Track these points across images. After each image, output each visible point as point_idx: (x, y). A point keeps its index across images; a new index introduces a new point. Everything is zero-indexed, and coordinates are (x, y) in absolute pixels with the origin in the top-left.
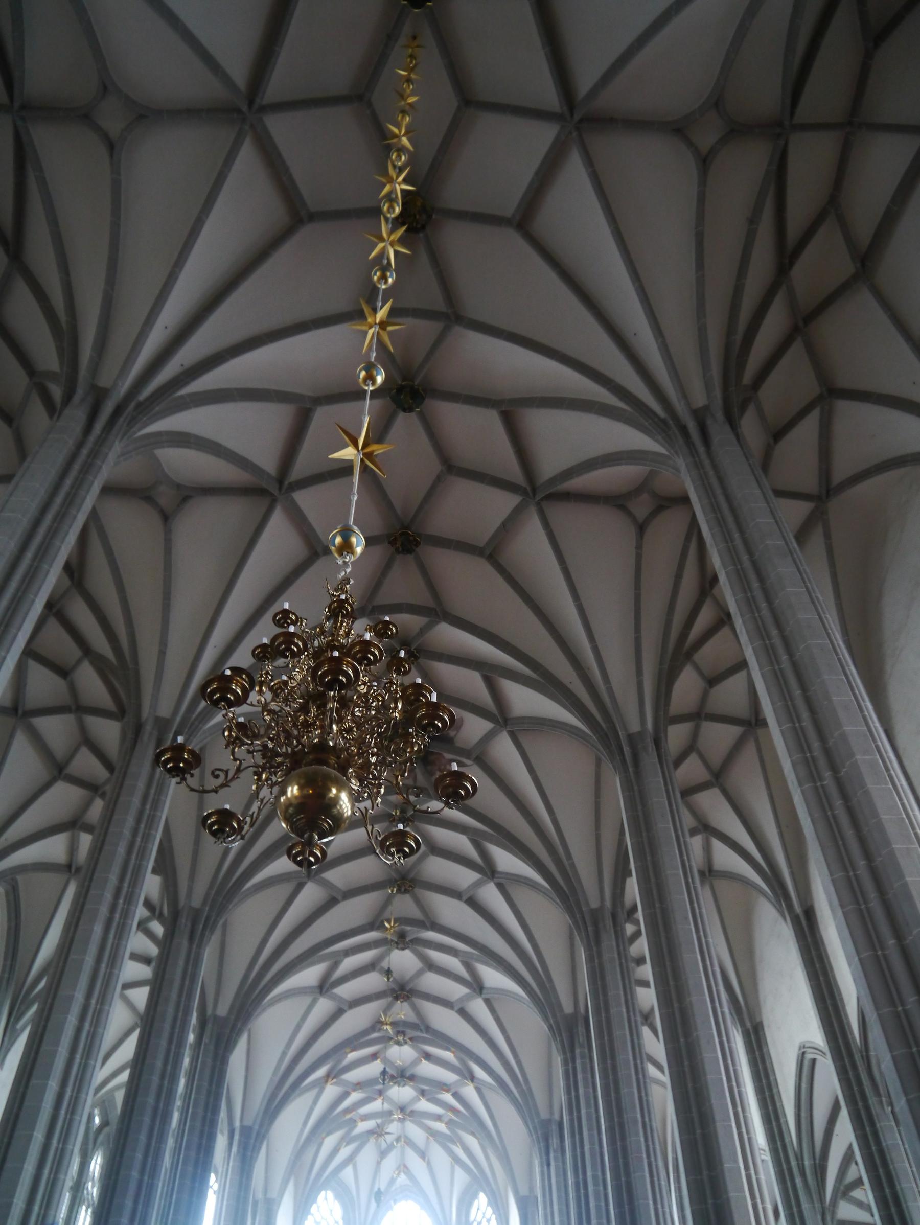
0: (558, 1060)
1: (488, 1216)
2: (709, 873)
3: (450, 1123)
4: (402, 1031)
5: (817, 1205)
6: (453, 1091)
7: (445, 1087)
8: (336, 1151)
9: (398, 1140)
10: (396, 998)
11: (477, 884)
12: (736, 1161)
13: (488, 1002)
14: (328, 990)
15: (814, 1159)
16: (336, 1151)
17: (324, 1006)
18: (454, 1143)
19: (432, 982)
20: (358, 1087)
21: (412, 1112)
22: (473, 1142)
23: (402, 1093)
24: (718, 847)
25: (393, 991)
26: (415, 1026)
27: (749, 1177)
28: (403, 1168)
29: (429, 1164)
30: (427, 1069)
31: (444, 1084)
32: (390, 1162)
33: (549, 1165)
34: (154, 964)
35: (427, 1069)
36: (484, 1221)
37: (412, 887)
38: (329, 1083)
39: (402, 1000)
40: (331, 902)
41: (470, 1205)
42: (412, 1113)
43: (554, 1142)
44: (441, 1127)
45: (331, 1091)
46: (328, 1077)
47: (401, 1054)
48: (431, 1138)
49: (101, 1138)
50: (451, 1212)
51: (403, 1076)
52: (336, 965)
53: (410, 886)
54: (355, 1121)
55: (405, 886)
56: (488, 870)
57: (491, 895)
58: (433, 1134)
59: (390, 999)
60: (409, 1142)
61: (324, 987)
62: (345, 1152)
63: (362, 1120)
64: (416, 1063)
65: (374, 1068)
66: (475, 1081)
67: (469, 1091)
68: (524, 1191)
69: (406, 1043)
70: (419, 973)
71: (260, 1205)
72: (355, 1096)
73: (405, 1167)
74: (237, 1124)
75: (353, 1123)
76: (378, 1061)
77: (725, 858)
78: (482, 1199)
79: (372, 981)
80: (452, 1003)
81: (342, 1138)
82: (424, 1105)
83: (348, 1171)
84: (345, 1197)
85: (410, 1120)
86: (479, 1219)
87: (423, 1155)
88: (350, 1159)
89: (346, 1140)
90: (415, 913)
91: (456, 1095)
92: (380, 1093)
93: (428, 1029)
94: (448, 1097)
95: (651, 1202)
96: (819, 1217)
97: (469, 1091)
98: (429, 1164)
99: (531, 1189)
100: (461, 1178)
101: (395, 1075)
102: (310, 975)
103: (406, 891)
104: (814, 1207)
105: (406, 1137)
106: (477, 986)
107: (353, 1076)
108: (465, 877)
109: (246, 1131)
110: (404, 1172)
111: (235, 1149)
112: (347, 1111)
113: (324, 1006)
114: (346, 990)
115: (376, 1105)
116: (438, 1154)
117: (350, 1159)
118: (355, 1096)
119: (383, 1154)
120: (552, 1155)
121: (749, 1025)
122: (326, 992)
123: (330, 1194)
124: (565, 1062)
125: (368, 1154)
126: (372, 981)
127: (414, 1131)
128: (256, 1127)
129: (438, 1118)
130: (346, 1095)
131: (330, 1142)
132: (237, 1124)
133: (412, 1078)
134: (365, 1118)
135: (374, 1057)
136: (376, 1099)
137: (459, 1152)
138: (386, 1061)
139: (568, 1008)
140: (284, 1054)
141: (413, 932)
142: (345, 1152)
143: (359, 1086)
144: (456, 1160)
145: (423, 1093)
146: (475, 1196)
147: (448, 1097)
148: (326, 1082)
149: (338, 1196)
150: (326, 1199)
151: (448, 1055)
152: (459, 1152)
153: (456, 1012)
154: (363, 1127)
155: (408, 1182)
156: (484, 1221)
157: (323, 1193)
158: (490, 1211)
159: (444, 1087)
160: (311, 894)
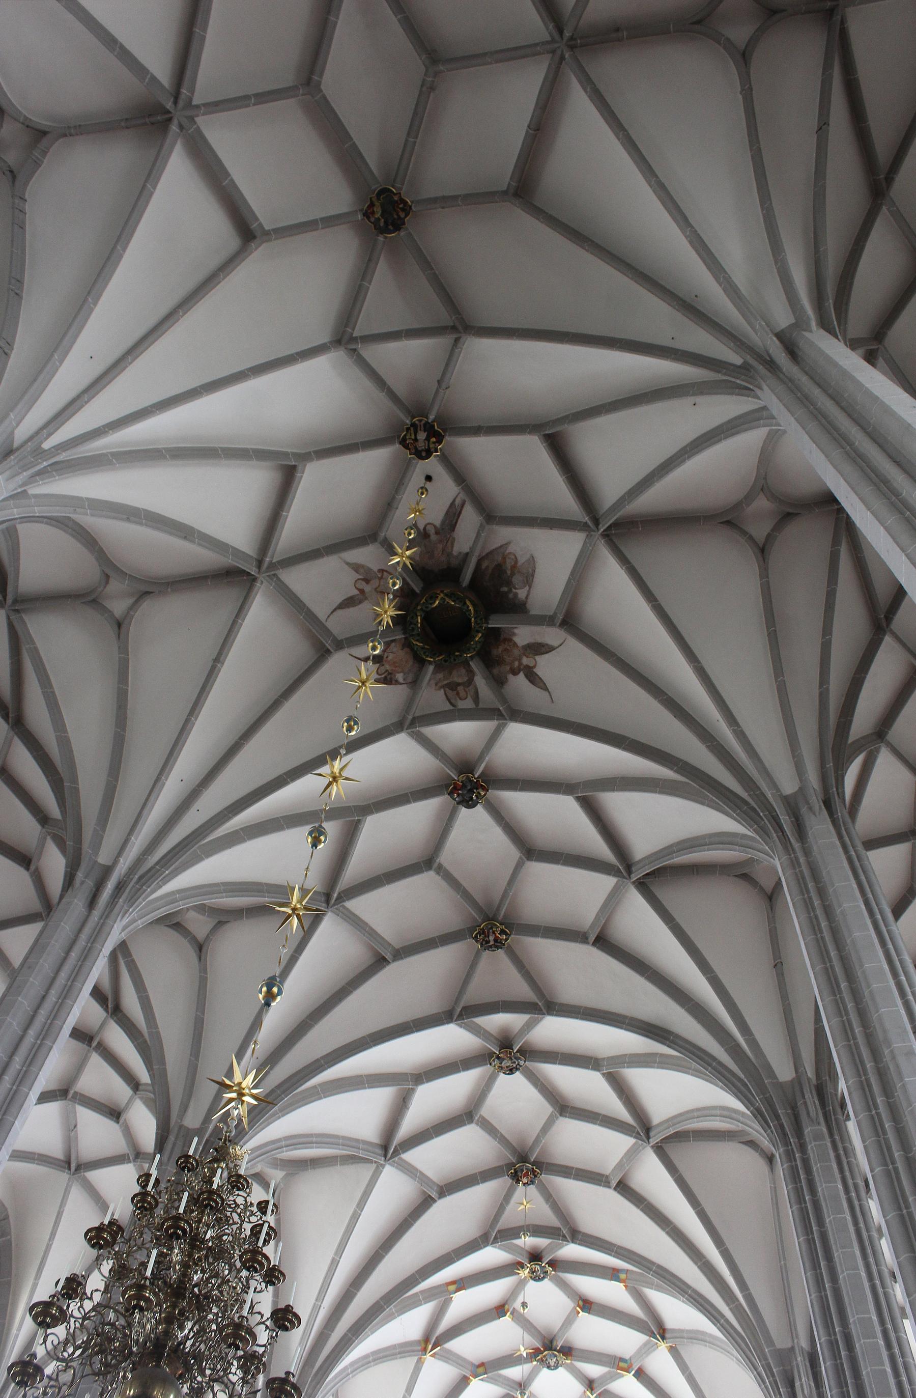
7: (622, 1364)
10: (516, 1178)
14: (396, 1152)
20: (481, 1370)
25: (510, 1165)
31: (621, 1360)
37: (506, 934)
38: (428, 1358)
39: (525, 1180)
53: (503, 932)
55: (494, 932)
59: (504, 1181)
66: (667, 1335)
76: (507, 1318)
80: (607, 1177)
103: (498, 944)
122: (393, 1156)
133: (568, 1351)
135: (500, 1310)
140: (334, 1264)
148: (424, 1350)
153: (615, 1189)
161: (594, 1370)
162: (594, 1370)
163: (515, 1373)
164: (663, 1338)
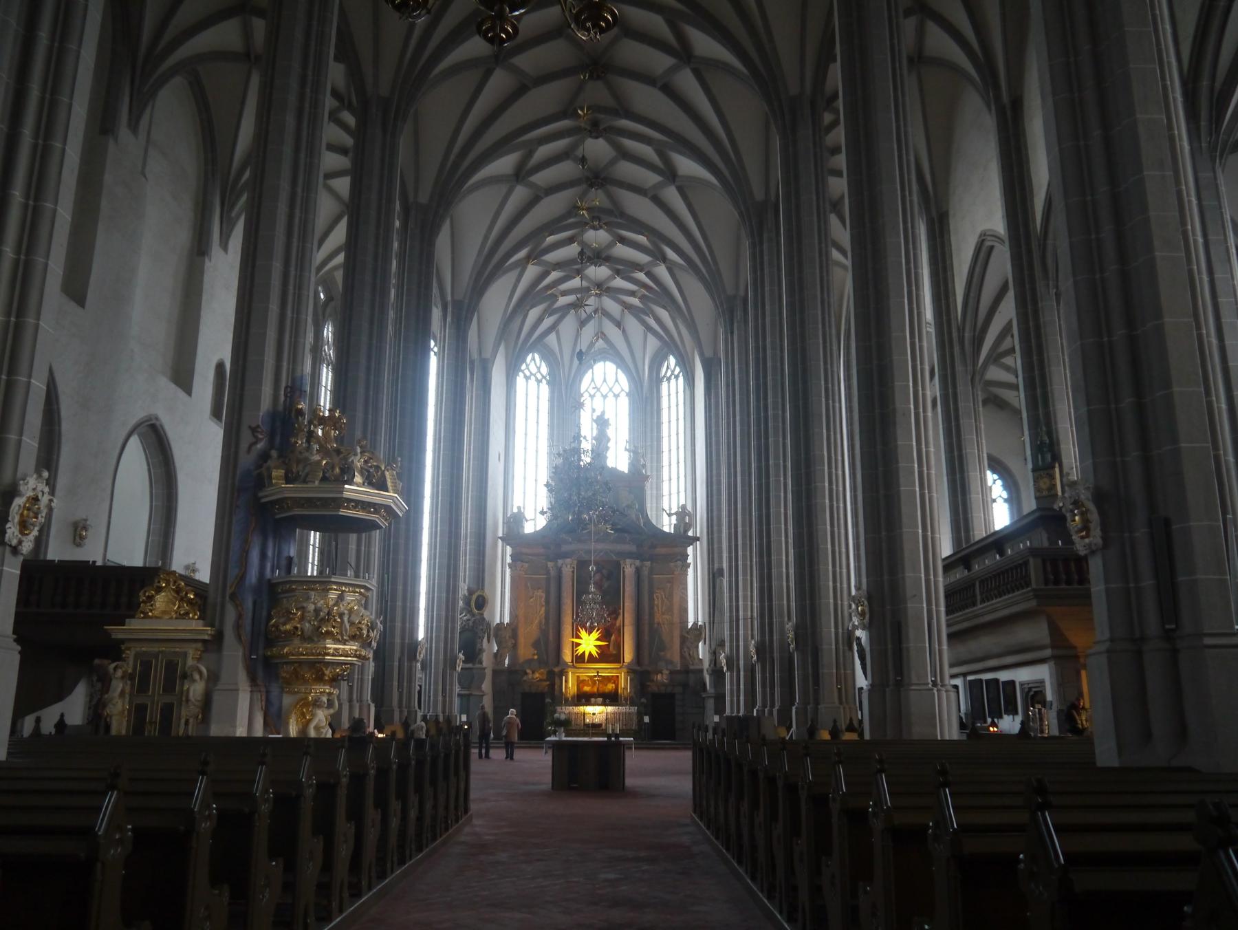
0: (746, 244)
1: (676, 373)
2: (919, 59)
3: (642, 298)
4: (598, 218)
5: (970, 368)
6: (647, 270)
8: (540, 320)
9: (596, 311)
10: (591, 186)
11: (673, 70)
12: (904, 331)
13: (681, 190)
15: (975, 331)
16: (540, 320)
17: (520, 193)
18: (648, 315)
19: (626, 170)
21: (608, 288)
22: (664, 314)
23: (599, 272)
24: (932, 28)
25: (588, 179)
26: (609, 212)
27: (913, 344)
28: (601, 335)
29: (624, 331)
30: (621, 251)
32: (589, 330)
33: (732, 333)
34: (351, 154)
35: (621, 251)
36: (673, 377)
40: (521, 90)
41: (661, 365)
42: (609, 290)
43: (739, 314)
44: (635, 301)
45: (532, 271)
46: (528, 258)
47: (597, 237)
48: (626, 310)
49: (329, 310)
50: (644, 370)
51: (599, 256)
52: (530, 154)
54: (556, 296)
56: (684, 54)
57: (687, 82)
58: (628, 307)
59: (584, 186)
60: (606, 314)
61: (520, 174)
62: (548, 322)
63: (562, 296)
64: (611, 245)
65: (573, 250)
67: (662, 271)
68: (709, 353)
69: (601, 227)
70: (613, 162)
71: (476, 364)
72: (554, 275)
73: (603, 333)
74: (449, 298)
75: (554, 298)
76: (575, 244)
77: (939, 42)
78: (672, 360)
79: (566, 169)
81: (545, 311)
82: (619, 282)
83: (552, 338)
84: (549, 356)
85: (606, 296)
87: (618, 324)
88: (553, 328)
89: (549, 312)
90: (609, 102)
91: (649, 274)
92: (579, 272)
93: (622, 214)
94: (641, 276)
95: (822, 363)
96: (969, 377)
97: (662, 271)
98: (624, 331)
99: (716, 352)
100: (653, 343)
101: (592, 257)
102: (504, 164)
103: (599, 78)
104: (966, 371)
105: (603, 309)
106: (671, 174)
107: (551, 257)
108: (660, 62)
109: (457, 305)
111: (449, 319)
112: (549, 287)
113: (520, 193)
114: (542, 178)
115: (576, 282)
116: (632, 323)
117: (553, 328)
118: (554, 275)
119: (582, 323)
120: (735, 325)
121: (934, 214)
123: (537, 356)
124: (753, 246)
125: (569, 323)
126: (566, 169)
127: (610, 304)
128: (467, 301)
129: (632, 294)
130: (545, 274)
131: (534, 313)
132: (449, 298)
134: (564, 293)
135: (571, 240)
136: (575, 278)
137: (652, 322)
138: (584, 245)
139: (759, 195)
140: (486, 238)
141: (607, 121)
142: (548, 322)
143: (558, 266)
144: (649, 328)
145: (618, 272)
146: (665, 358)
147: (641, 276)
148: (528, 262)
149: (543, 358)
150: (533, 359)
151: (642, 239)
152: (652, 322)
153: (650, 199)
154: (563, 301)
155: (605, 346)
156: (673, 377)
157: (531, 355)
158: (678, 370)
159: (638, 267)
160: (500, 81)
164: (664, 262)
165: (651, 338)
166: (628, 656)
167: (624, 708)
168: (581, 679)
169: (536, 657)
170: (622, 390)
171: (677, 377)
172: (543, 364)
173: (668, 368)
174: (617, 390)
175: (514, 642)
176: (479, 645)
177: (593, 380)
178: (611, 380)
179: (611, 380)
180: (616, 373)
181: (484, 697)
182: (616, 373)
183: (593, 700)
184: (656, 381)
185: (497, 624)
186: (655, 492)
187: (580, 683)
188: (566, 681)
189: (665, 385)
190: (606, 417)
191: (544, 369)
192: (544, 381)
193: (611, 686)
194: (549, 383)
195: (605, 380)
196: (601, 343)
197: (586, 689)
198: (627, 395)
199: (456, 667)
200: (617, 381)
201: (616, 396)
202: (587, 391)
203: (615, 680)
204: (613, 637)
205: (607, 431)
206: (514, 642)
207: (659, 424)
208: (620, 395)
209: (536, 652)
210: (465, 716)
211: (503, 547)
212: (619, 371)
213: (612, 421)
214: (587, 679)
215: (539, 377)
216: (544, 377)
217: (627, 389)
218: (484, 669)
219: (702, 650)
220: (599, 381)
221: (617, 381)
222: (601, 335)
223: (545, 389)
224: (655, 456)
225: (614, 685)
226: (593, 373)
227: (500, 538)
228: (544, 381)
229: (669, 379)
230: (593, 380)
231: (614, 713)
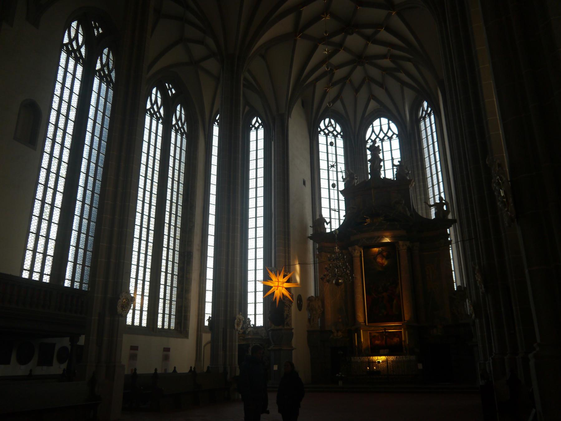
3: (393, 58)
28: (372, 97)
29: (387, 90)
32: (363, 94)
44: (387, 63)
63: (337, 69)
82: (374, 49)
86: (424, 115)
87: (382, 85)
88: (338, 97)
110: (372, 99)
115: (341, 56)
119: (357, 91)
129: (384, 57)
131: (320, 86)
137: (402, 76)
142: (333, 92)
144: (403, 83)
152: (402, 76)
154: (339, 74)
161: (369, 31)
162: (369, 31)
163: (337, 39)
165: (406, 89)
166: (407, 316)
167: (401, 357)
168: (373, 334)
169: (340, 320)
170: (394, 134)
171: (429, 115)
172: (337, 125)
173: (423, 111)
174: (390, 134)
175: (322, 309)
176: (286, 313)
177: (373, 131)
178: (385, 129)
179: (385, 129)
180: (389, 124)
181: (293, 351)
182: (389, 124)
183: (381, 351)
184: (416, 121)
185: (310, 297)
186: (423, 196)
187: (372, 338)
188: (359, 337)
189: (422, 124)
190: (376, 145)
191: (338, 129)
192: (339, 136)
193: (396, 340)
194: (342, 137)
195: (381, 130)
196: (373, 104)
197: (377, 342)
198: (398, 136)
199: (234, 326)
200: (389, 128)
201: (390, 138)
202: (370, 138)
203: (399, 334)
204: (395, 302)
205: (379, 155)
206: (322, 309)
207: (421, 149)
208: (393, 137)
209: (340, 316)
210: (277, 366)
211: (314, 244)
212: (390, 122)
213: (381, 148)
214: (377, 335)
215: (335, 133)
216: (338, 133)
217: (397, 133)
218: (292, 329)
219: (468, 307)
220: (377, 130)
221: (389, 128)
222: (372, 97)
223: (340, 142)
224: (420, 172)
225: (398, 339)
226: (373, 127)
227: (309, 237)
228: (339, 136)
229: (424, 118)
230: (373, 131)
231: (392, 361)
